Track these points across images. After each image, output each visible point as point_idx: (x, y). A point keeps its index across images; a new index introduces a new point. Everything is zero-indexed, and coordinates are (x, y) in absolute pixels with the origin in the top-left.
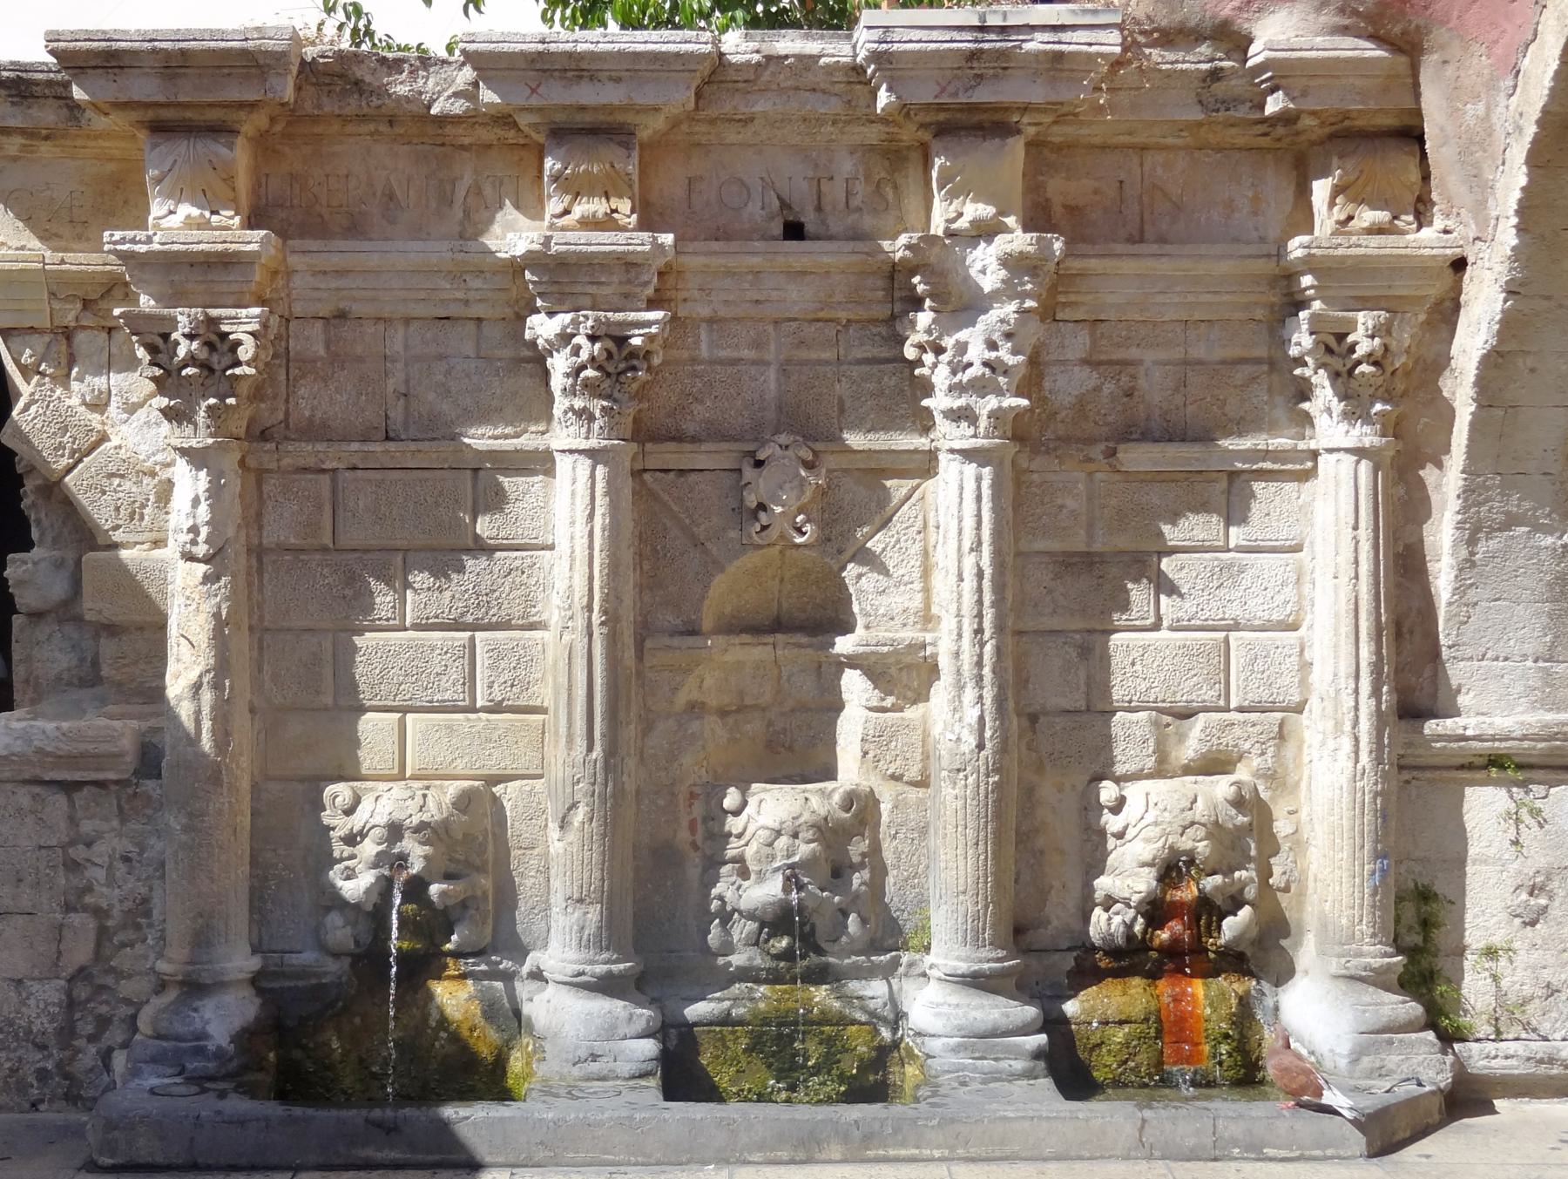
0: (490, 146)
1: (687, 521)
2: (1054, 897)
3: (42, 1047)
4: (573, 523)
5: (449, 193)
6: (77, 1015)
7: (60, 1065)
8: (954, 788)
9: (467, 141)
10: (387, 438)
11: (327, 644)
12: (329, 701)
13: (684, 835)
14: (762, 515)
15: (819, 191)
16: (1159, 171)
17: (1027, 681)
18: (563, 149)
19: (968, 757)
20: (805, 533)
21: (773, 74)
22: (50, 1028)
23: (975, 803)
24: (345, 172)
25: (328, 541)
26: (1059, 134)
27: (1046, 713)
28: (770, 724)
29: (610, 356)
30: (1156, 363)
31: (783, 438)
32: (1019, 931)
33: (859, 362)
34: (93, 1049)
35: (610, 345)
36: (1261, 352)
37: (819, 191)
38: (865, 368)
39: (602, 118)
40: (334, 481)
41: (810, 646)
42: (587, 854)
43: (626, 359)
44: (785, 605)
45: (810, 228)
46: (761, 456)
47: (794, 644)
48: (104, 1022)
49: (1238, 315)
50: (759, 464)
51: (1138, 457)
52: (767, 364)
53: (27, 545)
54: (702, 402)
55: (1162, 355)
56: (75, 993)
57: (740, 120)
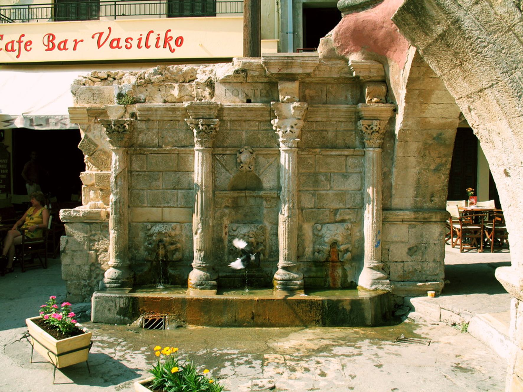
2: (307, 249)
3: (84, 280)
4: (198, 166)
6: (92, 273)
7: (89, 283)
10: (159, 147)
11: (145, 193)
12: (146, 205)
13: (224, 235)
14: (242, 165)
15: (254, 93)
16: (330, 89)
17: (301, 202)
22: (86, 276)
25: (145, 169)
26: (308, 80)
27: (305, 209)
29: (206, 129)
31: (246, 147)
32: (298, 257)
33: (264, 130)
34: (96, 280)
35: (206, 126)
37: (254, 93)
40: (147, 156)
43: (210, 129)
45: (252, 101)
46: (241, 151)
48: (98, 275)
50: (241, 153)
53: (84, 170)
54: (228, 139)
56: (92, 268)
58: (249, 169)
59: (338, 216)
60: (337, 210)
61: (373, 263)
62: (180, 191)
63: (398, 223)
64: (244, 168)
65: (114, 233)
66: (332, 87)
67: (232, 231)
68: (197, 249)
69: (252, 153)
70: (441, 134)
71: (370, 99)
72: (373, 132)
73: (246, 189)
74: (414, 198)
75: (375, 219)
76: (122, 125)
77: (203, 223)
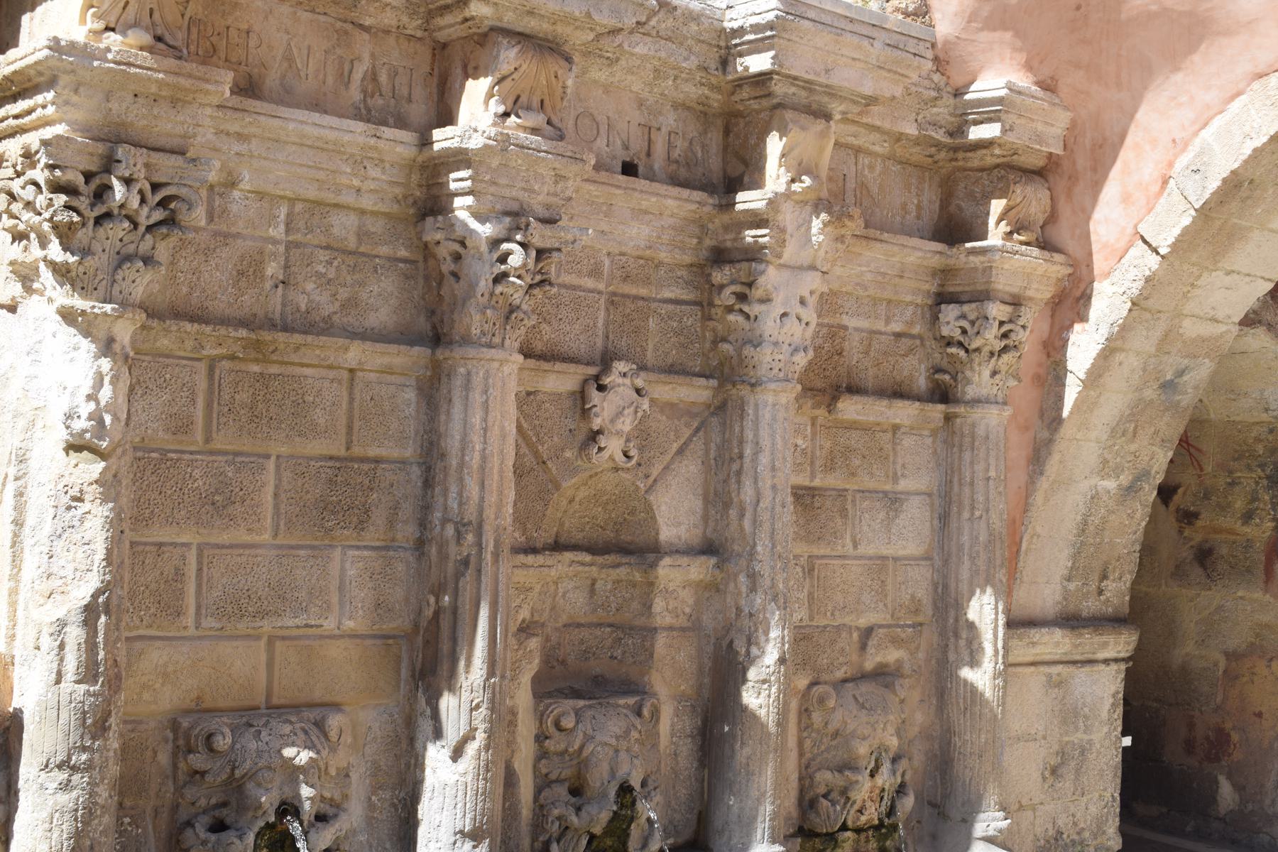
0: (387, 32)
1: (534, 439)
5: (346, 74)
8: (758, 697)
9: (368, 22)
16: (866, 172)
18: (515, 50)
19: (772, 669)
20: (632, 457)
21: (658, 22)
23: (776, 710)
24: (245, 26)
28: (548, 639)
30: (856, 329)
36: (916, 330)
38: (670, 307)
39: (545, 26)
41: (591, 565)
42: (481, 783)
44: (567, 525)
45: (641, 169)
47: (578, 562)
49: (909, 298)
50: (601, 388)
51: (850, 408)
52: (600, 293)
55: (864, 324)
57: (608, 58)
58: (620, 457)
59: (871, 650)
60: (868, 632)
61: (994, 820)
62: (351, 553)
63: (1020, 669)
64: (606, 454)
65: (65, 786)
66: (871, 168)
67: (557, 733)
68: (461, 832)
69: (638, 391)
70: (1181, 373)
71: (1008, 229)
72: (1005, 349)
73: (557, 546)
74: (1066, 583)
75: (1000, 661)
76: (155, 187)
77: (492, 709)
